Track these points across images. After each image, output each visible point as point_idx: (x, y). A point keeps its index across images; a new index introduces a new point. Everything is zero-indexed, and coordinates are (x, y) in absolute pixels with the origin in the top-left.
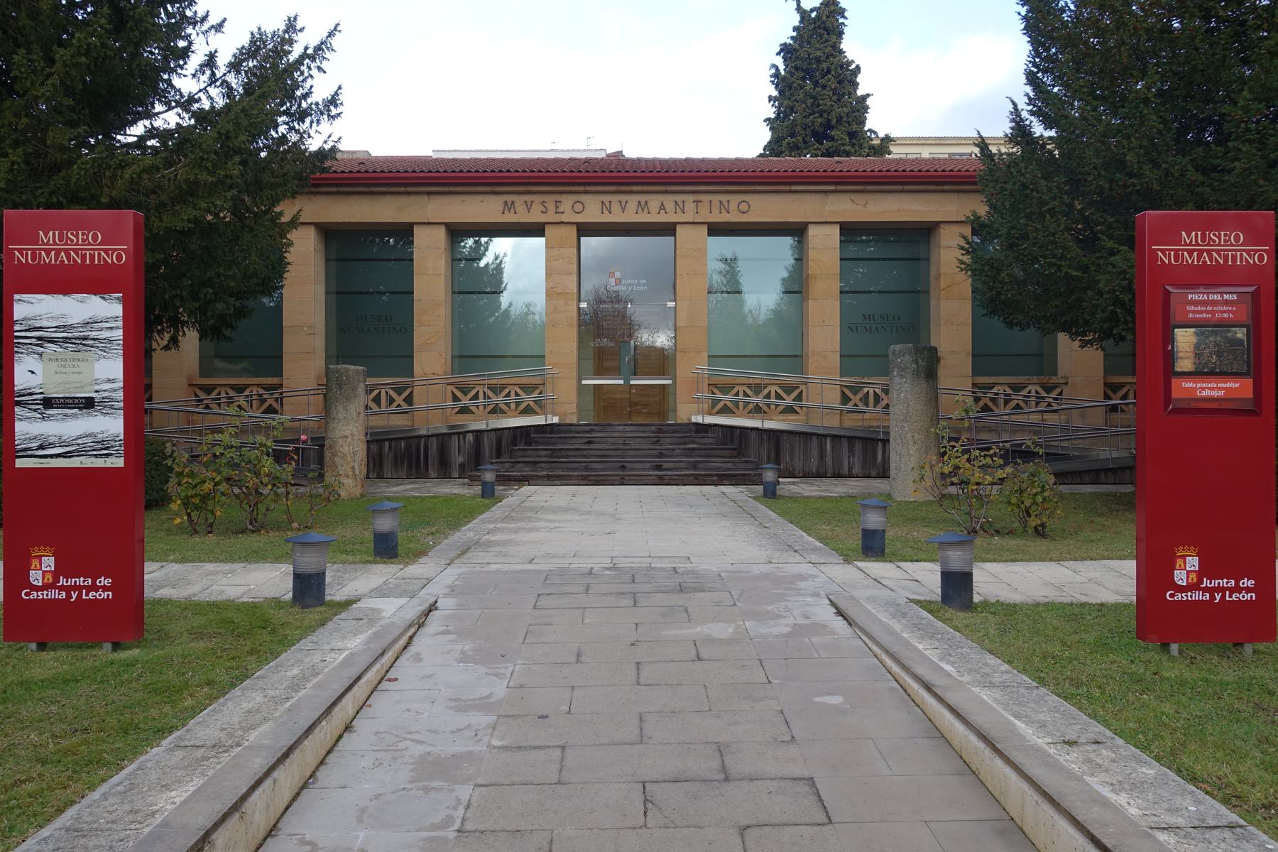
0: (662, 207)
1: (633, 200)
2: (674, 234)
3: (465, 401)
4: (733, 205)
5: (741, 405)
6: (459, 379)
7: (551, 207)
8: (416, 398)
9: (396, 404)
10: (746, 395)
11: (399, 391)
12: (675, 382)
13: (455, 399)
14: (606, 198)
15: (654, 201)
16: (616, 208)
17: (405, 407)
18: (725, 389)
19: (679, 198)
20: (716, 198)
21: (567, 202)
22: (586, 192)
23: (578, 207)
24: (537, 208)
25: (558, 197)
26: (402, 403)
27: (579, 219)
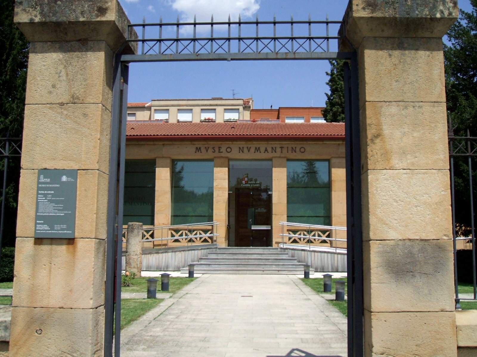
0: (266, 150)
2: (272, 161)
3: (177, 237)
5: (302, 239)
6: (176, 227)
8: (155, 235)
9: (146, 238)
10: (304, 235)
11: (147, 232)
12: (272, 227)
13: (173, 236)
17: (151, 239)
18: (295, 232)
23: (229, 150)
24: (210, 150)
26: (149, 237)
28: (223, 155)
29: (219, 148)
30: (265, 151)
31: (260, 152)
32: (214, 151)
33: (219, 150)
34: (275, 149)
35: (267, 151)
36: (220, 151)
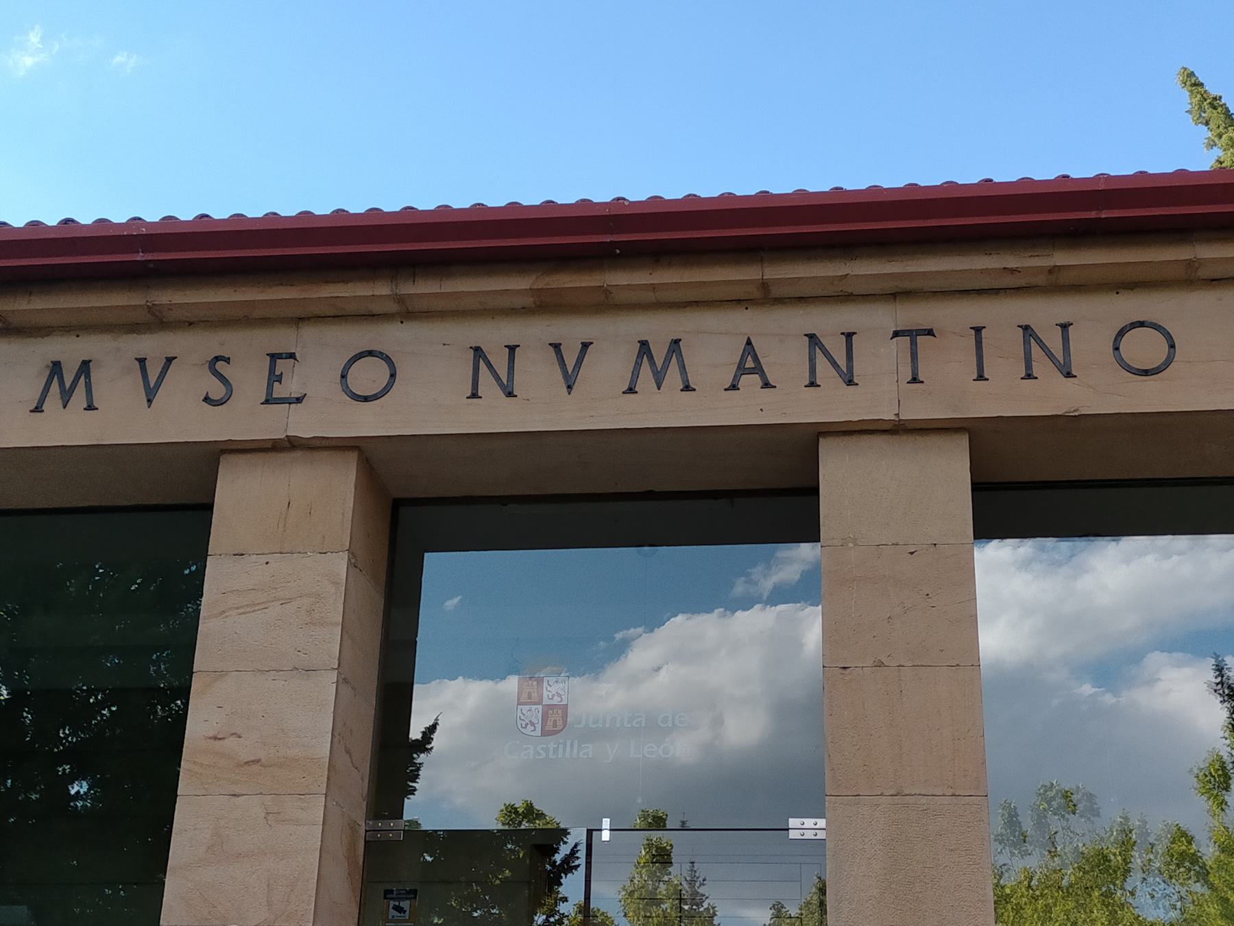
0: (750, 362)
1: (614, 338)
4: (1090, 344)
7: (249, 379)
14: (493, 335)
15: (712, 340)
16: (535, 372)
19: (829, 321)
20: (1000, 316)
21: (319, 356)
22: (407, 313)
23: (368, 376)
25: (282, 338)
27: (368, 423)
28: (301, 423)
29: (274, 357)
30: (742, 370)
31: (687, 388)
32: (218, 391)
33: (275, 378)
34: (842, 363)
35: (758, 369)
36: (279, 391)
